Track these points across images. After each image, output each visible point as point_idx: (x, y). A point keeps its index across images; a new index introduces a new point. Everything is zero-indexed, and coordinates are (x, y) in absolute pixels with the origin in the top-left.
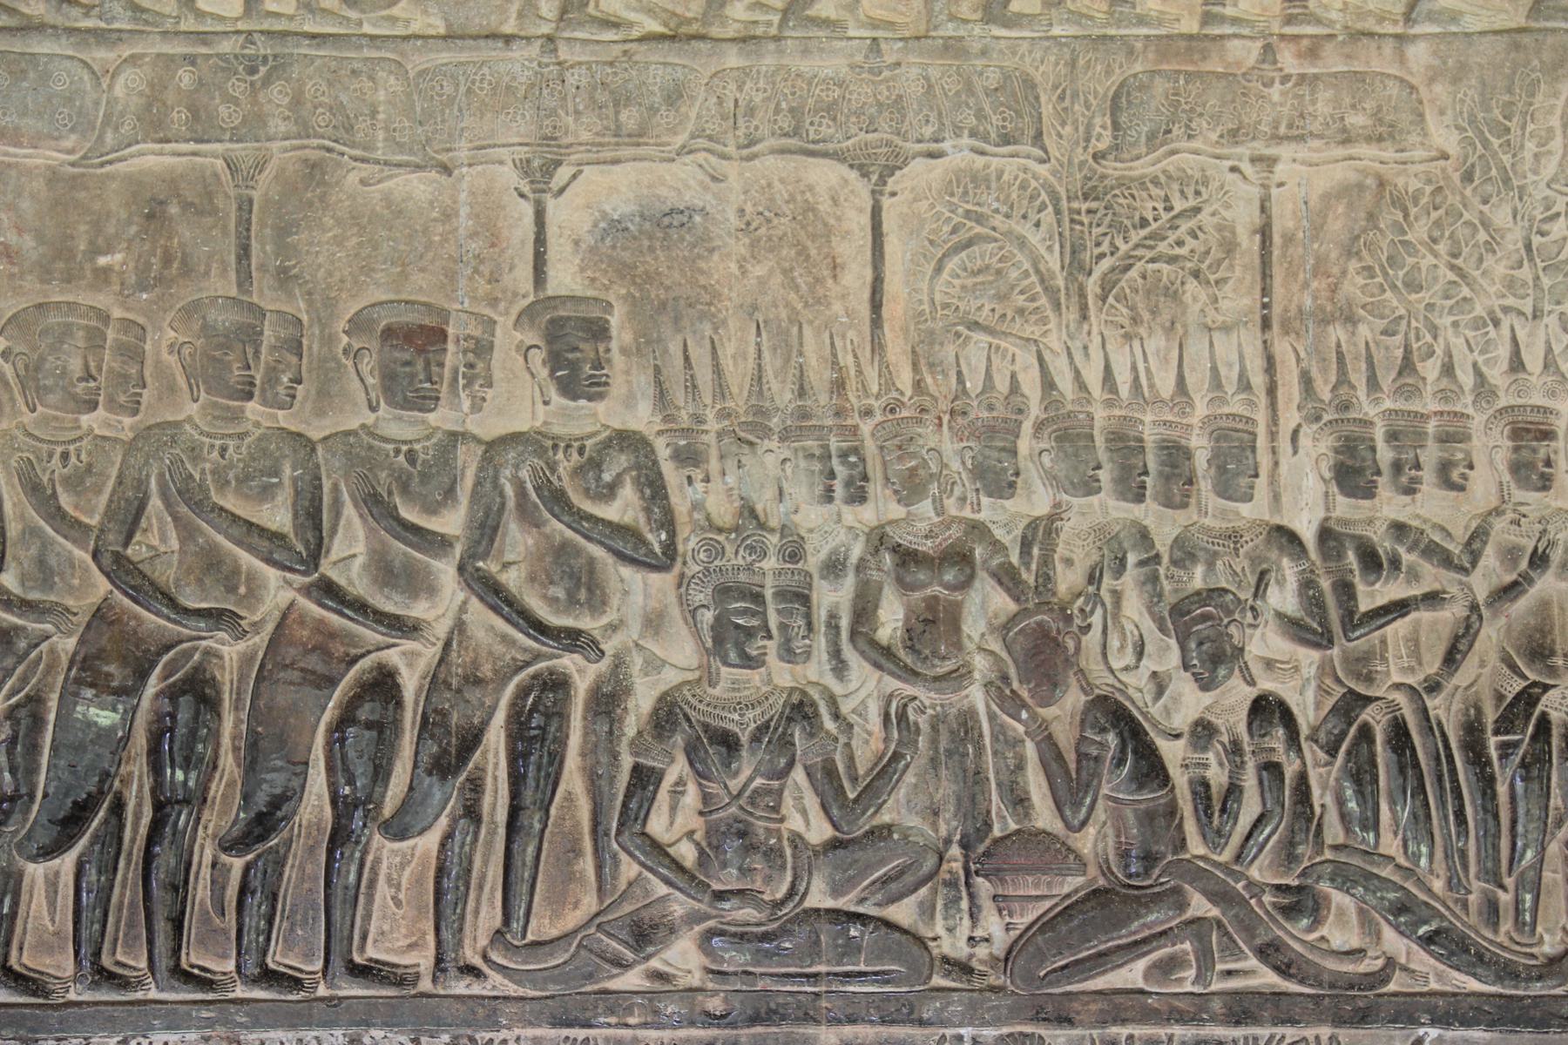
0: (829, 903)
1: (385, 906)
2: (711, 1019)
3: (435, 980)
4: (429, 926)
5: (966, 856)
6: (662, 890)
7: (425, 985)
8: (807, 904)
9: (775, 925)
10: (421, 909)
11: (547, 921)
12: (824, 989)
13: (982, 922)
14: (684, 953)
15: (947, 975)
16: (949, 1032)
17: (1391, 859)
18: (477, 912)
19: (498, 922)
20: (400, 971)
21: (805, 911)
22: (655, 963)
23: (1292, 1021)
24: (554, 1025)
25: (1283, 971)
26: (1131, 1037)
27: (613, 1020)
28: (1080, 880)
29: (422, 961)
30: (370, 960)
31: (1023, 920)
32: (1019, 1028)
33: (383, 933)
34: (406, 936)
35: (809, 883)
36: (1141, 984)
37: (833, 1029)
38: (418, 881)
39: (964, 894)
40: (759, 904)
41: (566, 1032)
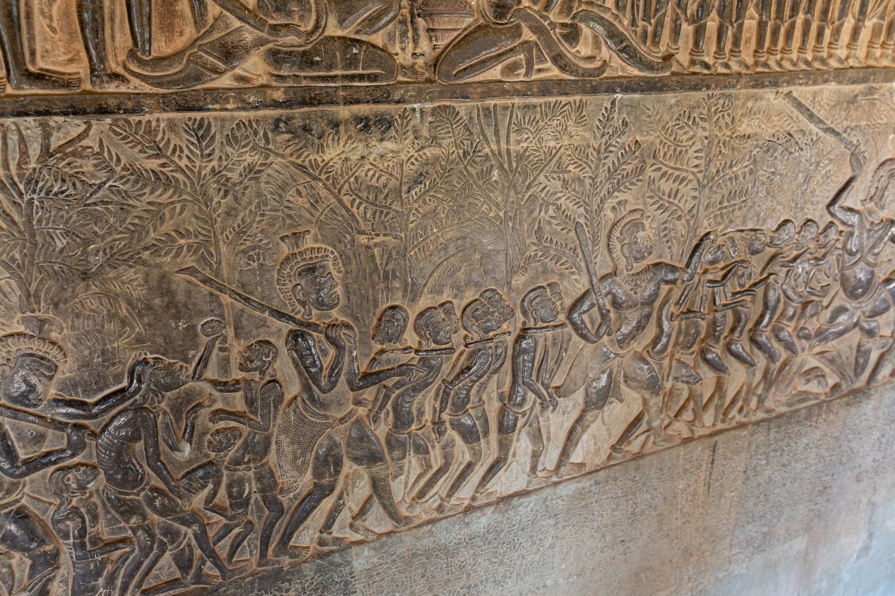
0: (339, 33)
1: (43, 32)
2: (276, 104)
3: (92, 82)
4: (80, 46)
5: (412, 5)
6: (237, 24)
7: (88, 86)
8: (326, 34)
9: (310, 46)
10: (71, 34)
11: (164, 44)
12: (340, 84)
13: (420, 45)
14: (255, 64)
15: (405, 75)
16: (408, 106)
17: (610, 9)
18: (113, 37)
19: (130, 44)
20: (66, 77)
21: (326, 38)
22: (238, 71)
23: (566, 94)
24: (178, 110)
25: (563, 68)
26: (495, 105)
27: (217, 106)
28: (471, 20)
29: (81, 71)
30: (42, 69)
31: (442, 43)
32: (443, 103)
33: (47, 51)
34: (65, 53)
35: (326, 20)
36: (499, 78)
37: (347, 107)
38: (66, 14)
39: (410, 28)
40: (299, 34)
41: (188, 115)
